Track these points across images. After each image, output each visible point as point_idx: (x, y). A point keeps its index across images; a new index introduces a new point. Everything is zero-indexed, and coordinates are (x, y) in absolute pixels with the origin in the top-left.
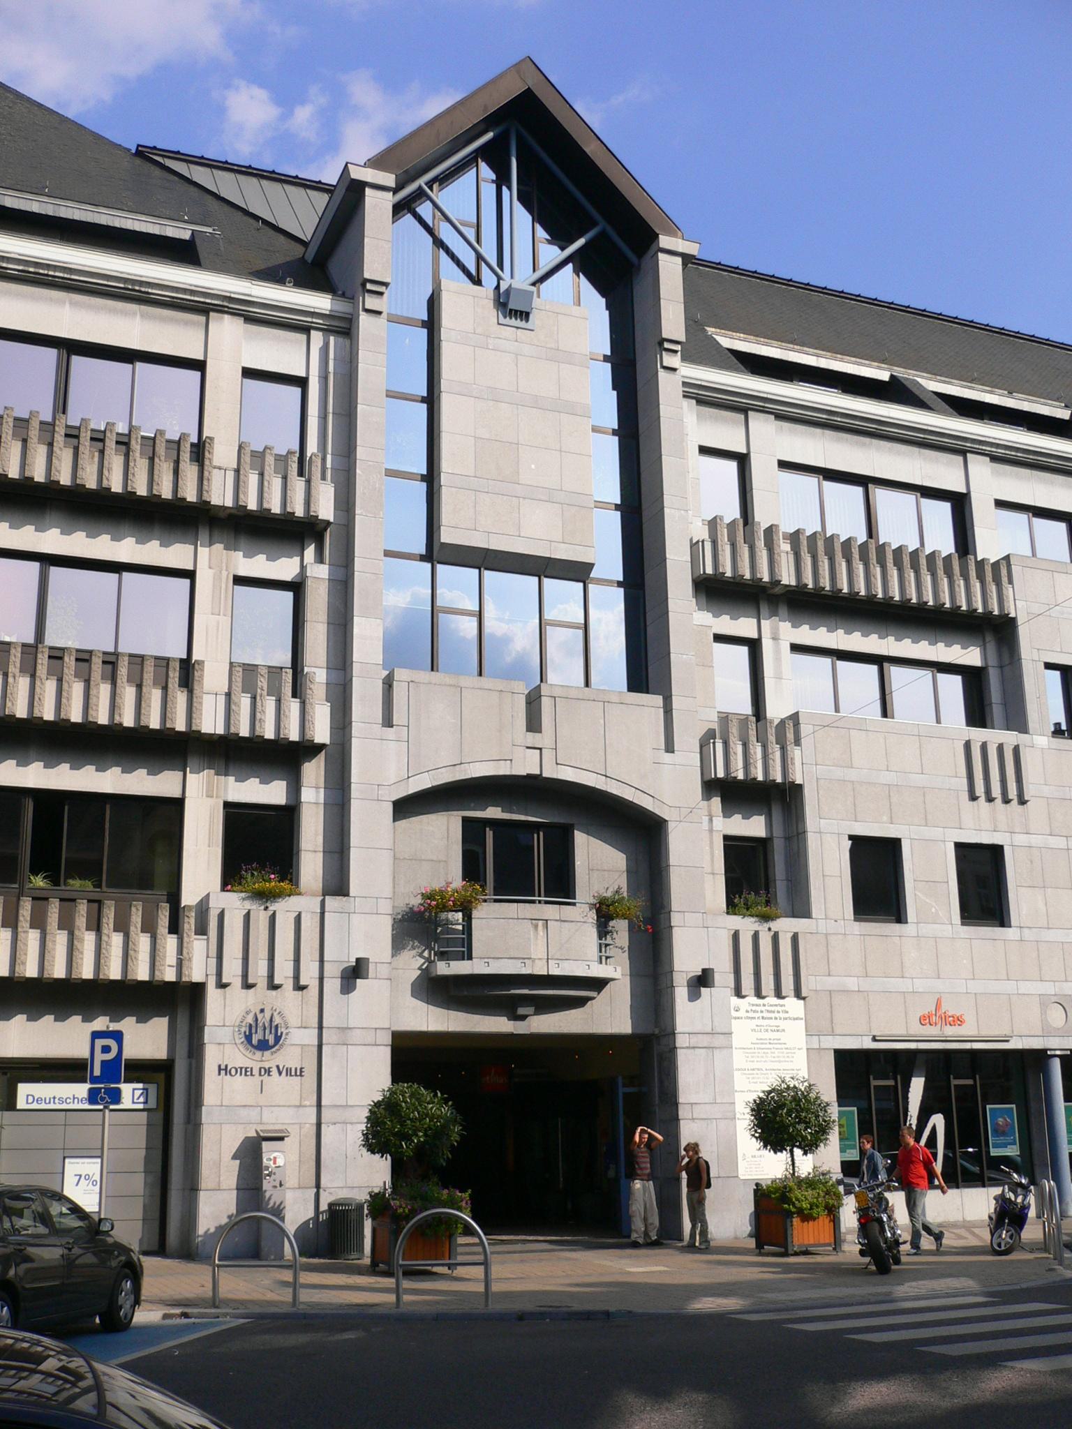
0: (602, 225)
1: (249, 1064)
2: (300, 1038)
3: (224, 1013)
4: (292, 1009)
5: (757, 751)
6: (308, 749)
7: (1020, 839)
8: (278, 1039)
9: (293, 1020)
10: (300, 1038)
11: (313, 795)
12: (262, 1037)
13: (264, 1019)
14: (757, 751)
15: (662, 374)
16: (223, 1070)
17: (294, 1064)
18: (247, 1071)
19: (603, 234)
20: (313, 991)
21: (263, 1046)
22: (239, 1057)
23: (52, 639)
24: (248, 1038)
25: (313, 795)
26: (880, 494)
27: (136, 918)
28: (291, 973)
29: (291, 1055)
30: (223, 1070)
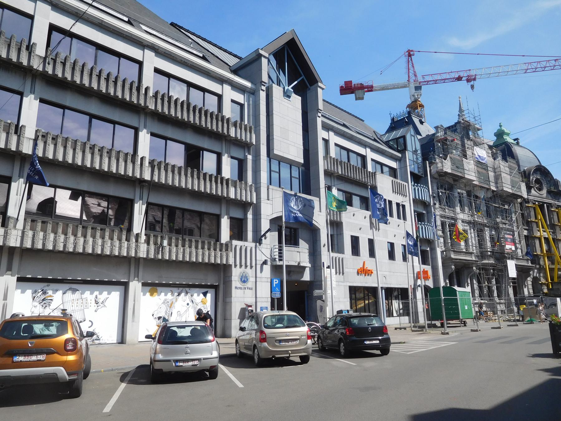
0: (303, 77)
1: (241, 286)
2: (252, 279)
3: (236, 273)
4: (250, 272)
5: (244, 192)
6: (251, 204)
7: (378, 238)
8: (247, 280)
9: (250, 275)
10: (252, 279)
11: (250, 216)
12: (244, 279)
13: (244, 275)
14: (244, 192)
15: (318, 118)
16: (236, 288)
17: (250, 287)
18: (241, 288)
19: (303, 79)
20: (254, 268)
21: (244, 282)
22: (239, 284)
23: (117, 147)
24: (241, 280)
25: (250, 216)
26: (351, 154)
27: (70, 230)
28: (233, 261)
29: (251, 283)
30: (236, 288)
